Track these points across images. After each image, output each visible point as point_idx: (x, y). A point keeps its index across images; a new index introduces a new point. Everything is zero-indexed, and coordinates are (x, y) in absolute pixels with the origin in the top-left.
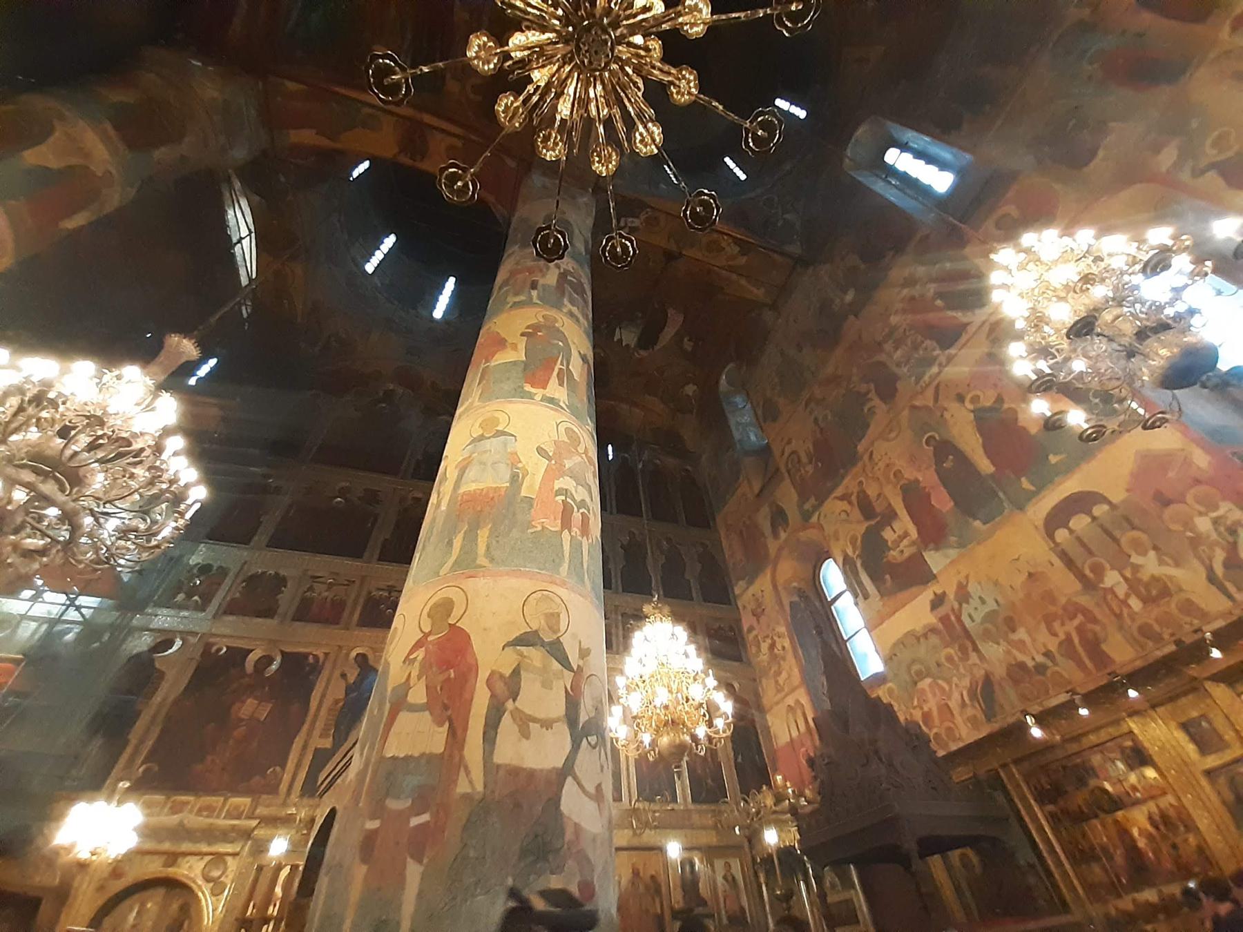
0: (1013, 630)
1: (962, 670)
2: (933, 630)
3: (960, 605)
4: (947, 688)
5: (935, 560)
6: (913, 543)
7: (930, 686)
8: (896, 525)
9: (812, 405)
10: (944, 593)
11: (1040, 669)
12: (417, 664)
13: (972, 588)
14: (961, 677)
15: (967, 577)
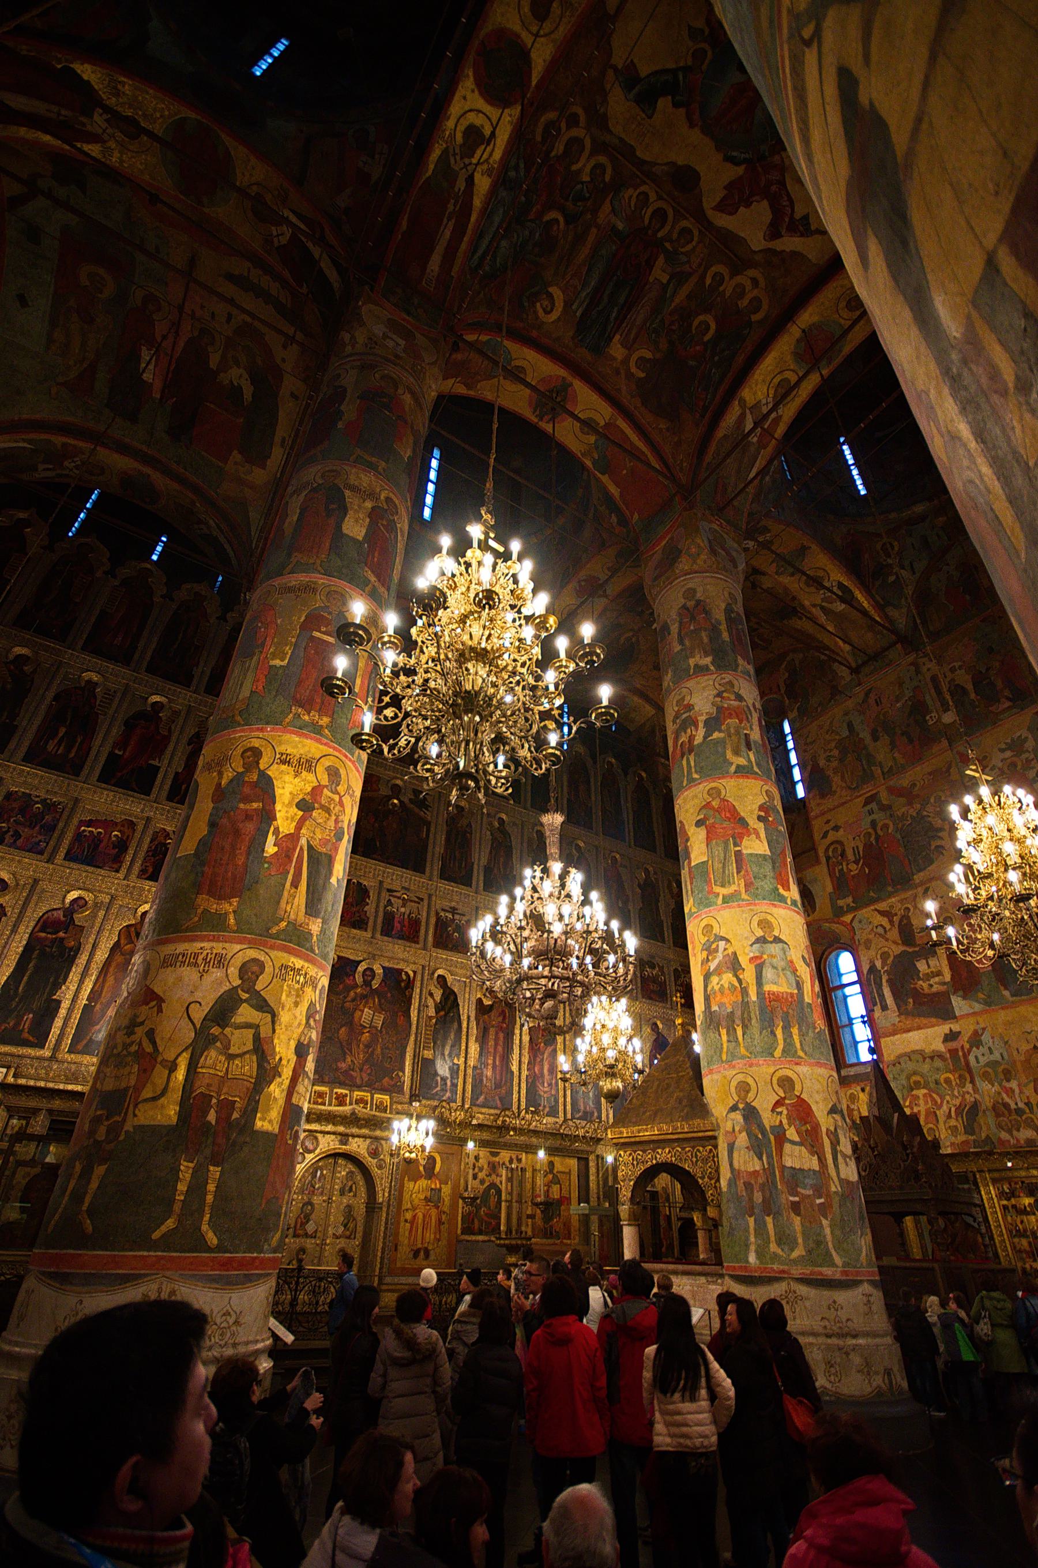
0: (1008, 1081)
1: (956, 1093)
2: (940, 1056)
3: (971, 1047)
4: (939, 1101)
5: (959, 1004)
6: (944, 983)
7: (925, 1095)
8: (933, 962)
9: (874, 806)
10: (960, 1032)
11: (1019, 1112)
12: (784, 1116)
13: (986, 1038)
14: (953, 1096)
15: (984, 1029)
